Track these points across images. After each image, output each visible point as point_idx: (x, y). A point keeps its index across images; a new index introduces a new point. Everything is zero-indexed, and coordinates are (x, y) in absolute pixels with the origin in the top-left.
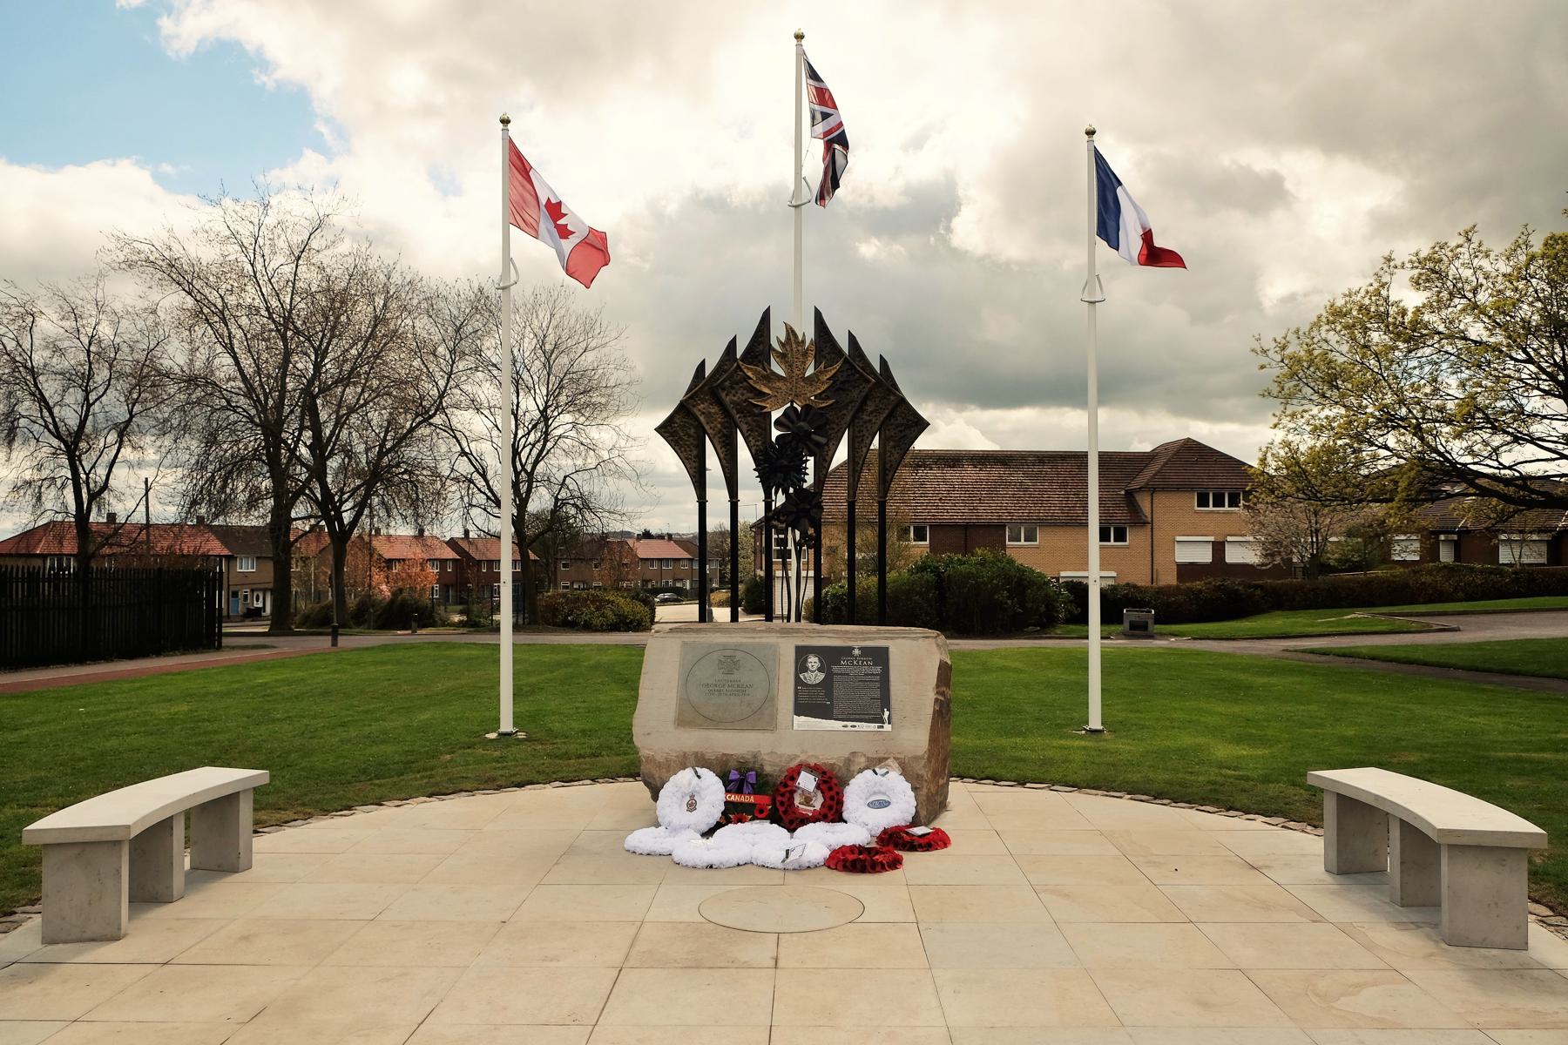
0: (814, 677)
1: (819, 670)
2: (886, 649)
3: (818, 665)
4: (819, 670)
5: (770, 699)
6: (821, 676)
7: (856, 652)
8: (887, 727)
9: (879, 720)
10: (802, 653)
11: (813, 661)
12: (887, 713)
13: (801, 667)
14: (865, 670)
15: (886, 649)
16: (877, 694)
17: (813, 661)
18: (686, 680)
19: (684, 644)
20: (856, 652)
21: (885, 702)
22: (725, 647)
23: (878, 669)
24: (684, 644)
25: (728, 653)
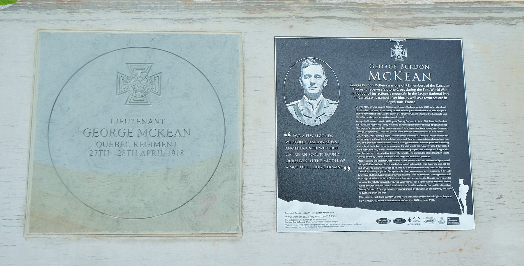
0: (316, 110)
1: (327, 92)
2: (454, 48)
3: (321, 82)
4: (327, 92)
5: (226, 163)
6: (331, 108)
7: (399, 52)
8: (464, 217)
9: (449, 205)
10: (291, 53)
11: (313, 74)
12: (464, 189)
13: (289, 88)
14: (416, 91)
15: (454, 48)
16: (443, 145)
17: (313, 74)
18: (47, 124)
19: (44, 36)
20: (399, 52)
21: (461, 167)
22: (128, 43)
23: (442, 91)
24: (44, 36)
25: (138, 56)
